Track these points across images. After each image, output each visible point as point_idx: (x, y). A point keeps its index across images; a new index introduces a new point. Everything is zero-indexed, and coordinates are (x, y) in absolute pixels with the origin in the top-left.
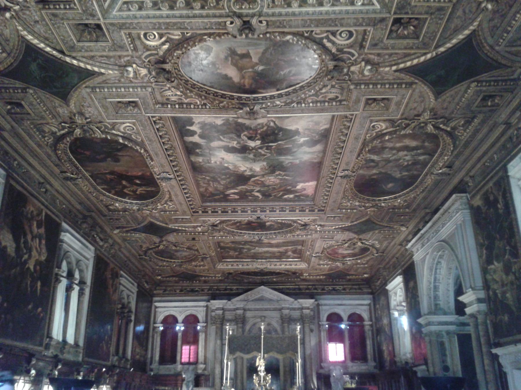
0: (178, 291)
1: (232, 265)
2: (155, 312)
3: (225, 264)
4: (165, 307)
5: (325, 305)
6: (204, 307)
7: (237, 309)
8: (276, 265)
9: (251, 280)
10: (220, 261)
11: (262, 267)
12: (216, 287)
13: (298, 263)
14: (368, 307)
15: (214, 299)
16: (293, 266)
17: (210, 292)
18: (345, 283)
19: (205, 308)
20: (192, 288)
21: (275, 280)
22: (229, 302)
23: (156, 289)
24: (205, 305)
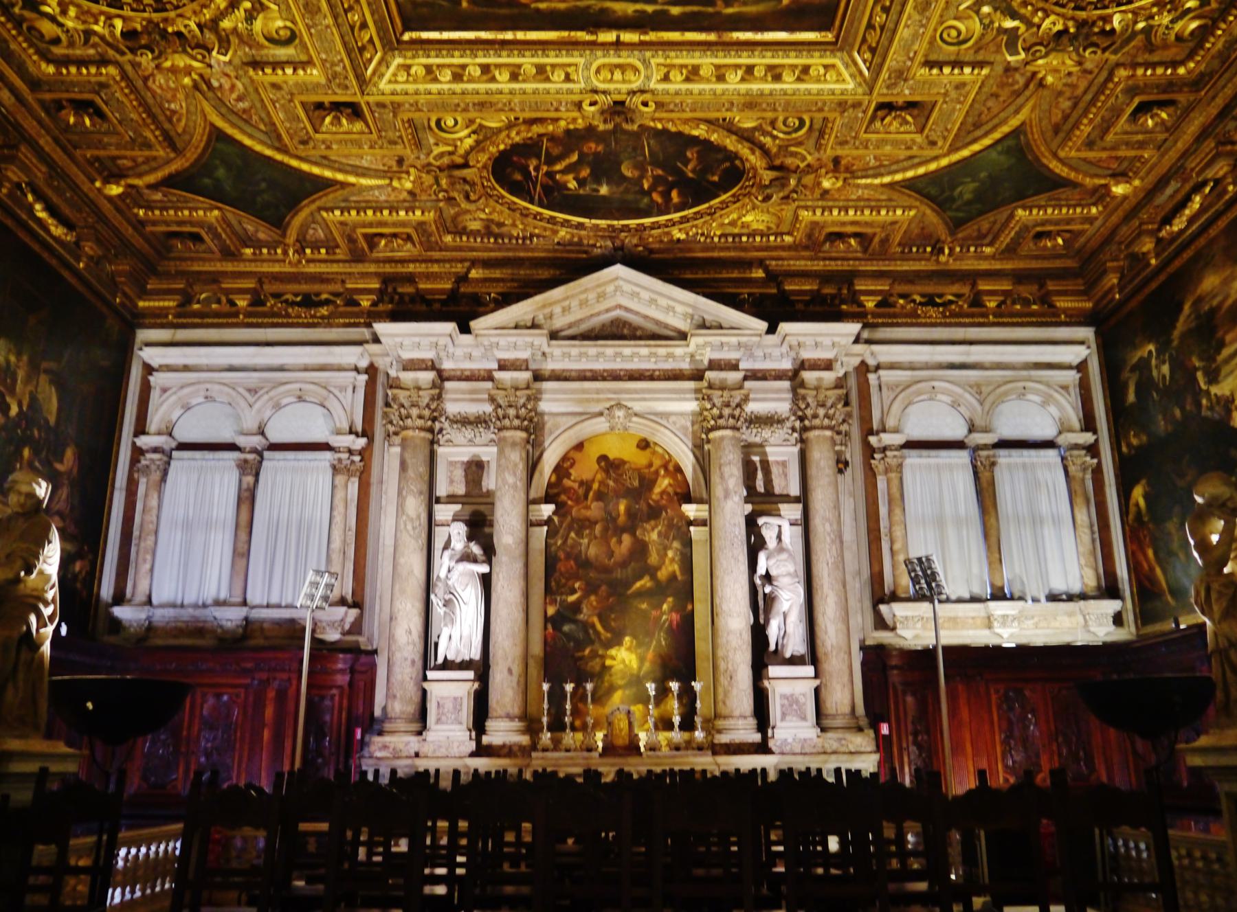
0: (242, 303)
1: (457, 77)
2: (146, 389)
3: (419, 63)
4: (186, 368)
5: (892, 366)
6: (356, 369)
7: (503, 366)
8: (693, 74)
9: (563, 233)
10: (392, 45)
11: (619, 86)
12: (408, 289)
13: (816, 61)
14: (1072, 377)
15: (396, 316)
16: (789, 84)
17: (381, 307)
18: (984, 266)
19: (364, 377)
20: (305, 288)
21: (678, 234)
22: (466, 338)
23: (144, 293)
24: (364, 364)
